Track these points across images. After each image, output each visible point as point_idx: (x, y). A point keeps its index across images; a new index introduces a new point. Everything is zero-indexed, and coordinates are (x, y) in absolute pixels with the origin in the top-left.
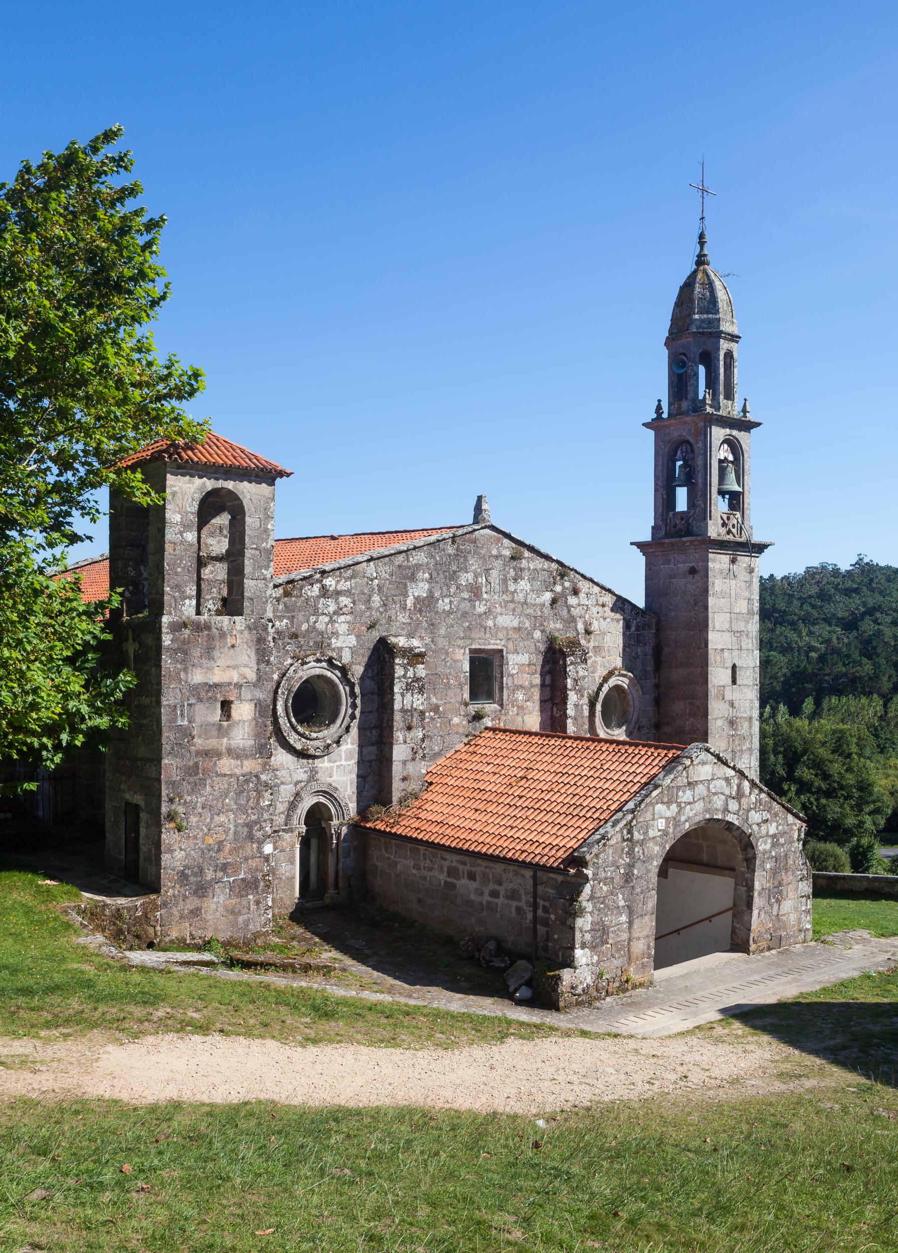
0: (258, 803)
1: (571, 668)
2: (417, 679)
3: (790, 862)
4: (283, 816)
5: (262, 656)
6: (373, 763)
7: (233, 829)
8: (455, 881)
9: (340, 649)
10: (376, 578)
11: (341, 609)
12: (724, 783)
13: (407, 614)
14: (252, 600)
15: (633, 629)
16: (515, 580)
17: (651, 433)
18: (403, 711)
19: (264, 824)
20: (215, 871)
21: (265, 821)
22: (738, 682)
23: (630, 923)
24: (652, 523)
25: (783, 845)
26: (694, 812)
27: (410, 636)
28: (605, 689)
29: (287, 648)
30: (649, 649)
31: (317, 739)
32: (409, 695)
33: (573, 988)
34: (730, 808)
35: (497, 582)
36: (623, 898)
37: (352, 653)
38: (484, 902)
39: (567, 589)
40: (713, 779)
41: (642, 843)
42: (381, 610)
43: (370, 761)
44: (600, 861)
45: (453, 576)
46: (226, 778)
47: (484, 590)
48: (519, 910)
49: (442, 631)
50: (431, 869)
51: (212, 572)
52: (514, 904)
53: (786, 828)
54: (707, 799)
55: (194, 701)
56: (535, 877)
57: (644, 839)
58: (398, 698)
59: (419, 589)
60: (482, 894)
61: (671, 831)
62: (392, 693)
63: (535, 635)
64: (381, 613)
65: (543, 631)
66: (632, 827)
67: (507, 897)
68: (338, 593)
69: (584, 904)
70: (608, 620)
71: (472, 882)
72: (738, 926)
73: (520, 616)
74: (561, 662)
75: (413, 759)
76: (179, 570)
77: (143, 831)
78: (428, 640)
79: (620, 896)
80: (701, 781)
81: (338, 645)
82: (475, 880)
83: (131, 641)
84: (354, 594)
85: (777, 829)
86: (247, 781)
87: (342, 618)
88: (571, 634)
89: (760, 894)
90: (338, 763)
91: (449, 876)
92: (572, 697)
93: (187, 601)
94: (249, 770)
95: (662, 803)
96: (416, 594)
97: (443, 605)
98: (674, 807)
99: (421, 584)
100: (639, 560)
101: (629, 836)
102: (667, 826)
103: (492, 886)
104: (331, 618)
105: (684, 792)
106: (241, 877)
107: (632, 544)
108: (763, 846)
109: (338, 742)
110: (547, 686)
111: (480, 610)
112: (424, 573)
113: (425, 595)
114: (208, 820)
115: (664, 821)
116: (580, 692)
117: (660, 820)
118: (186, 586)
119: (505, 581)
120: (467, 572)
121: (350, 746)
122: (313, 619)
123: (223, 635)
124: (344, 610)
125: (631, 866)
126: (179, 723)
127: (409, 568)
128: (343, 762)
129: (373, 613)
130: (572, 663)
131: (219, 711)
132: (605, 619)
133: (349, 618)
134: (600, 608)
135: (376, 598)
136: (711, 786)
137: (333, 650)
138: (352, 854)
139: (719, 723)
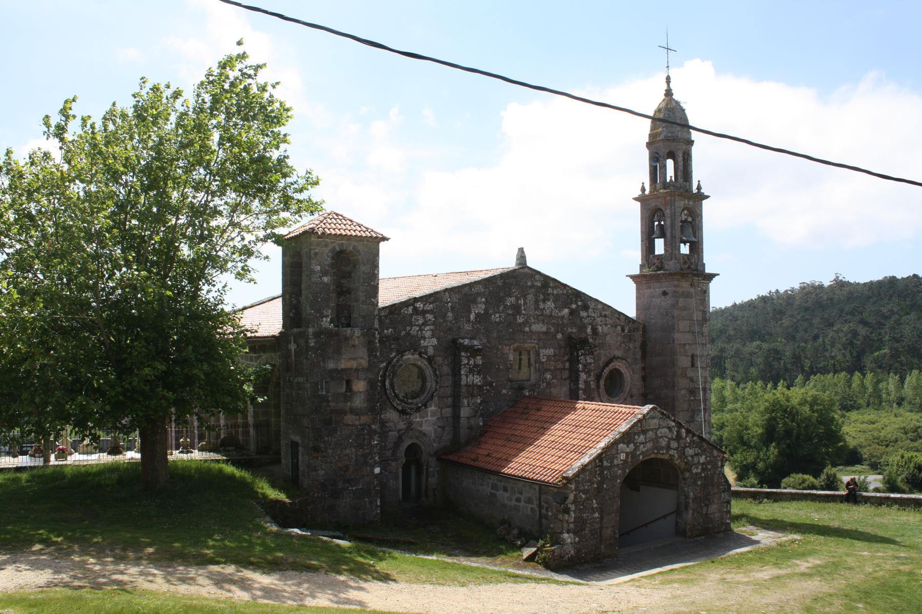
0: (370, 443)
1: (582, 357)
2: (476, 366)
3: (716, 480)
4: (391, 451)
5: (371, 350)
6: (449, 419)
7: (354, 458)
8: (496, 492)
9: (427, 347)
10: (450, 302)
11: (427, 322)
12: (667, 430)
13: (471, 324)
14: (365, 317)
15: (626, 331)
16: (544, 301)
17: (638, 204)
18: (467, 385)
19: (374, 455)
20: (344, 483)
21: (375, 453)
23: (601, 518)
24: (640, 263)
25: (710, 470)
26: (646, 448)
27: (472, 339)
28: (607, 370)
29: (392, 346)
30: (638, 344)
31: (411, 403)
32: (471, 376)
33: (561, 557)
34: (672, 446)
35: (531, 303)
36: (596, 503)
37: (434, 349)
38: (513, 505)
39: (580, 306)
40: (659, 428)
41: (608, 468)
42: (453, 322)
43: (447, 418)
44: (580, 479)
45: (501, 300)
46: (350, 427)
47: (523, 308)
48: (532, 509)
49: (495, 335)
50: (482, 485)
51: (344, 300)
52: (530, 506)
53: (712, 459)
54: (656, 440)
55: (329, 380)
56: (540, 489)
57: (611, 466)
58: (464, 377)
59: (479, 308)
60: (511, 500)
61: (630, 460)
62: (460, 375)
63: (558, 337)
64: (453, 324)
65: (563, 334)
66: (602, 458)
67: (526, 502)
68: (424, 312)
69: (569, 506)
70: (609, 326)
71: (505, 493)
72: (680, 521)
73: (548, 324)
74: (575, 354)
75: (475, 416)
76: (319, 300)
77: (300, 458)
78: (485, 341)
79: (594, 501)
80: (651, 430)
81: (425, 344)
82: (507, 491)
83: (292, 343)
84: (435, 312)
85: (706, 459)
86: (363, 429)
87: (428, 328)
88: (583, 336)
89: (693, 500)
90: (426, 419)
91: (492, 489)
92: (583, 376)
93: (324, 319)
94: (364, 422)
96: (477, 312)
97: (496, 318)
98: (632, 446)
99: (480, 306)
100: (632, 286)
101: (600, 464)
102: (627, 457)
103: (517, 495)
104: (420, 327)
105: (639, 436)
106: (360, 487)
107: (627, 276)
109: (425, 406)
110: (567, 369)
111: (519, 321)
112: (482, 298)
113: (482, 312)
114: (339, 452)
115: (625, 454)
116: (588, 373)
117: (622, 454)
118: (324, 310)
119: (537, 302)
120: (511, 297)
121: (433, 408)
122: (408, 328)
123: (347, 339)
124: (429, 322)
125: (601, 483)
126: (320, 393)
127: (472, 295)
128: (429, 418)
129: (448, 324)
130: (582, 355)
131: (344, 386)
132: (606, 325)
133: (432, 327)
134: (603, 319)
135: (450, 314)
136: (658, 432)
137: (422, 347)
138: (436, 475)
139: (683, 392)
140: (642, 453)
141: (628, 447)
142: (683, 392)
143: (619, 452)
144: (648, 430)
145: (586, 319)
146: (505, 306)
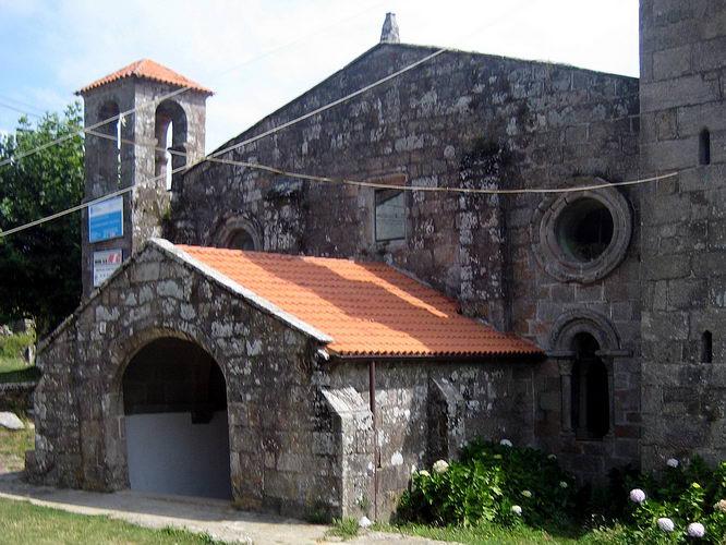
9: (250, 203)
16: (418, 95)
22: (713, 158)
26: (139, 317)
34: (183, 315)
40: (160, 280)
47: (380, 116)
81: (249, 200)
85: (264, 347)
95: (103, 305)
96: (310, 139)
97: (338, 142)
98: (116, 313)
105: (127, 295)
108: (232, 369)
132: (559, 111)
140: (134, 324)
141: (111, 313)
142: (667, 231)
143: (97, 319)
144: (141, 284)
145: (504, 107)
146: (352, 120)
